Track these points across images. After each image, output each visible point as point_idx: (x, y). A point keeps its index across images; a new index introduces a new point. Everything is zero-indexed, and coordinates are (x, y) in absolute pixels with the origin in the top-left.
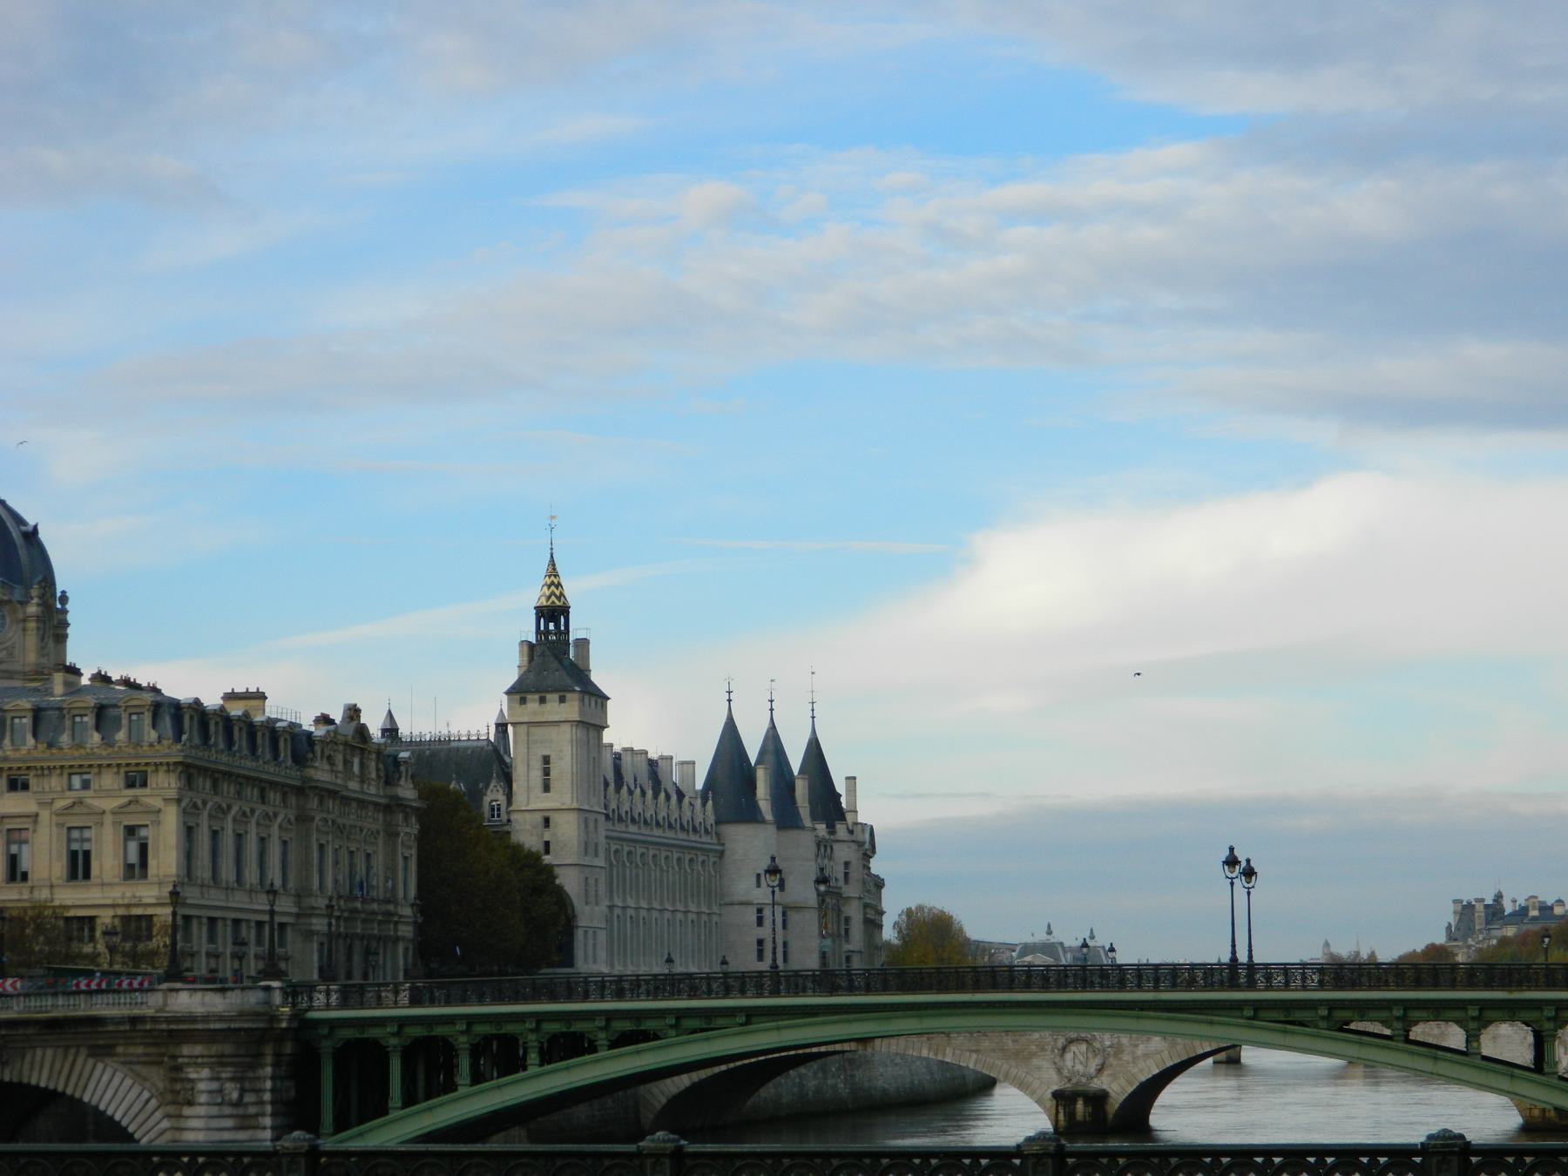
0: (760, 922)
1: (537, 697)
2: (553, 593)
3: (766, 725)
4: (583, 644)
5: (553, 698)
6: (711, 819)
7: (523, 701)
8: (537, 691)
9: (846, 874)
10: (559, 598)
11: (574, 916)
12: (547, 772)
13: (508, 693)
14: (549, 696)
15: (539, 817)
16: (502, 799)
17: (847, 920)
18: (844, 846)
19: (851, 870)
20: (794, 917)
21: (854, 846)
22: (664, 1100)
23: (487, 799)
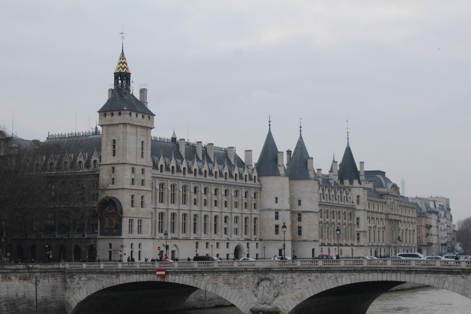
0: (277, 218)
1: (110, 113)
2: (121, 67)
3: (298, 137)
4: (143, 91)
5: (116, 113)
6: (255, 174)
7: (105, 115)
8: (110, 111)
10: (123, 69)
11: (122, 212)
12: (114, 146)
13: (99, 112)
14: (114, 113)
15: (110, 167)
16: (98, 159)
17: (358, 219)
18: (357, 189)
20: (304, 216)
21: (362, 189)
22: (76, 304)
23: (92, 160)
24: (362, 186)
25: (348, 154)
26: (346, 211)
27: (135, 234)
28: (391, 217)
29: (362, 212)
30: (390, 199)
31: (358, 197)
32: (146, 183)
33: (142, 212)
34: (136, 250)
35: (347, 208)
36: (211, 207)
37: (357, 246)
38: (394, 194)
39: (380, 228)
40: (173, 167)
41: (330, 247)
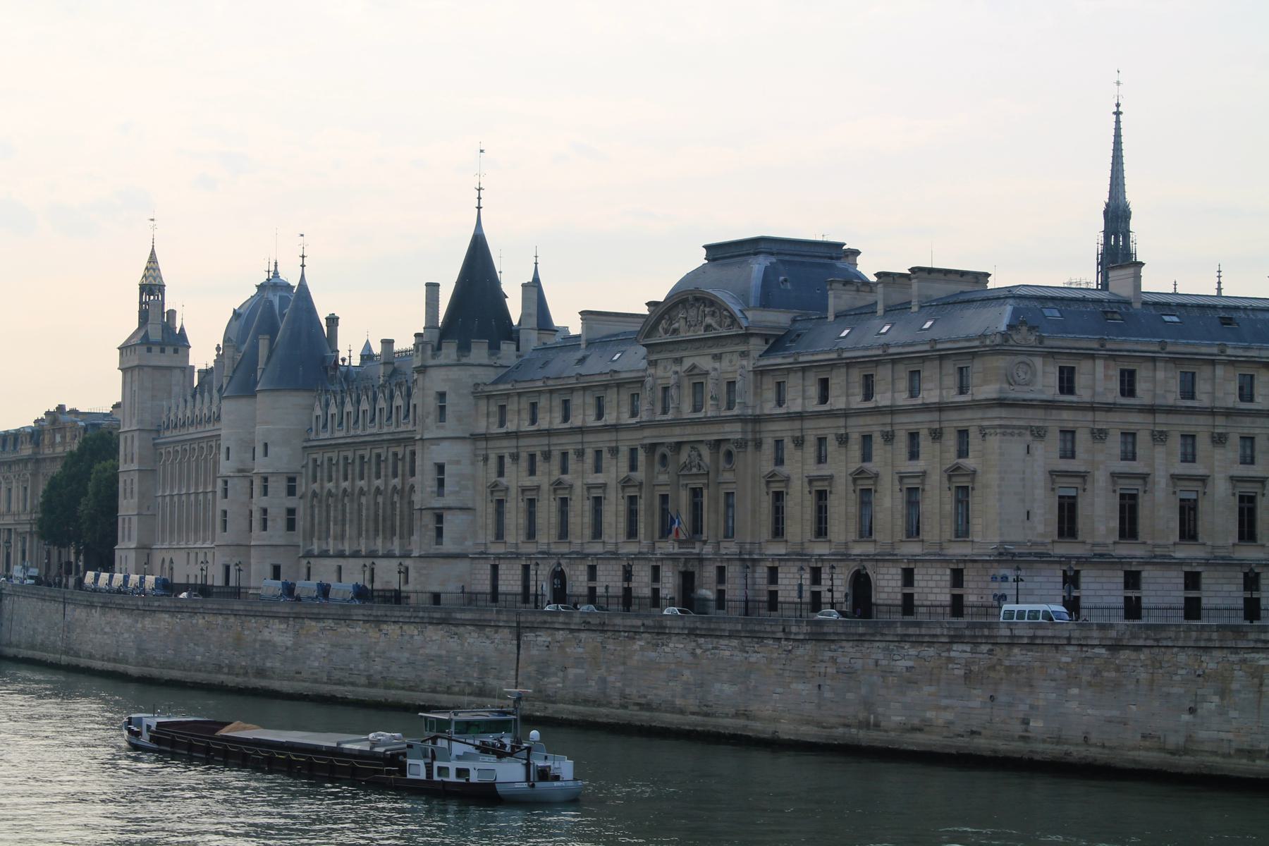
30: (679, 361)
39: (604, 486)
41: (341, 562)
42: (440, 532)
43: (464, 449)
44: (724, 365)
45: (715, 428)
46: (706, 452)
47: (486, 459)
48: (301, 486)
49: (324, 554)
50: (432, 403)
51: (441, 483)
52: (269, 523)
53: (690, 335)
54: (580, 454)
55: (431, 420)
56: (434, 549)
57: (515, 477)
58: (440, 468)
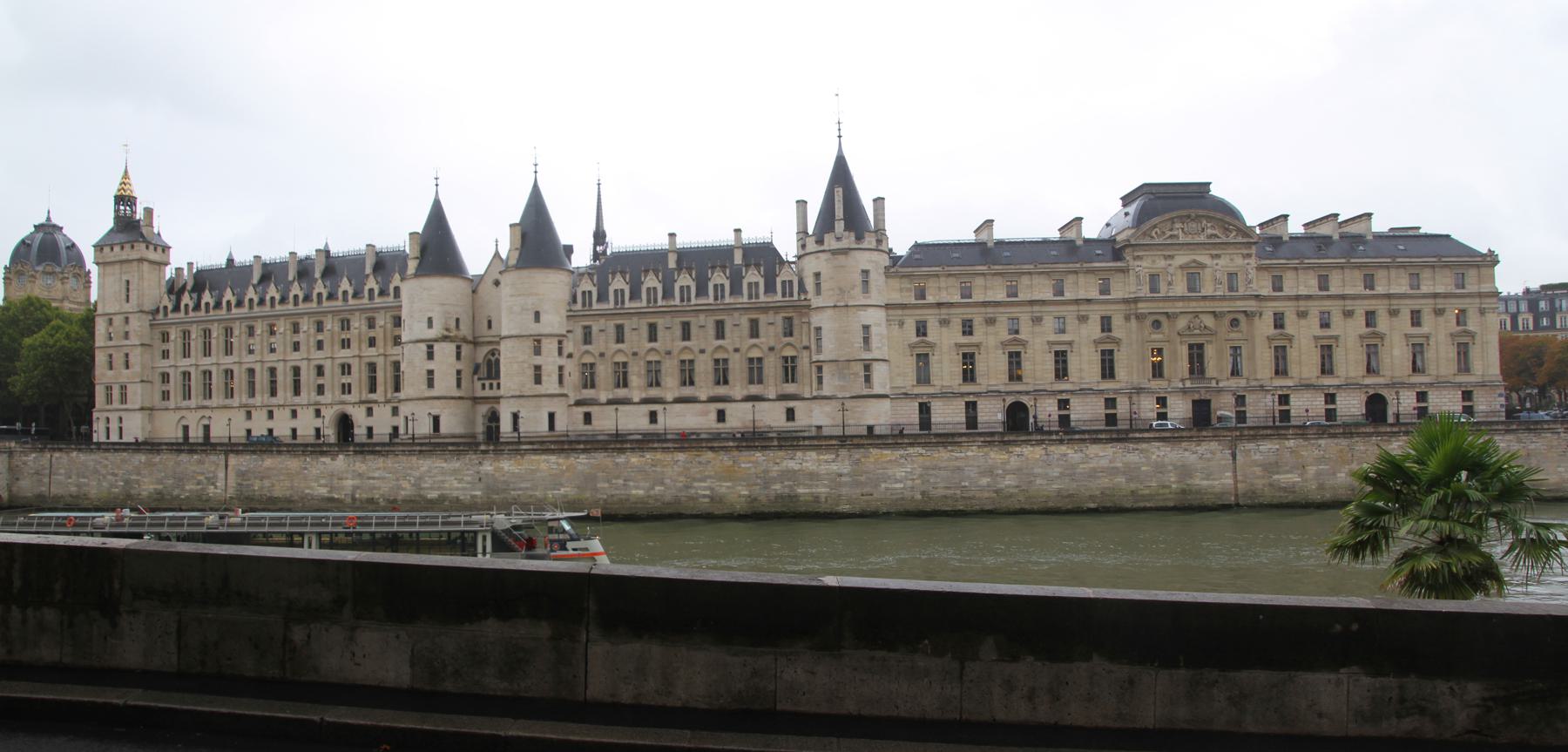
9: (818, 285)
17: (818, 329)
19: (823, 277)
24: (825, 247)
25: (841, 175)
26: (763, 319)
27: (116, 405)
28: (1143, 308)
29: (830, 312)
31: (817, 275)
32: (131, 335)
33: (125, 375)
34: (114, 426)
35: (765, 309)
36: (285, 352)
37: (815, 398)
38: (1202, 239)
39: (1070, 343)
40: (251, 300)
42: (868, 379)
43: (882, 314)
44: (1222, 262)
45: (1225, 303)
46: (1209, 321)
47: (901, 324)
48: (569, 347)
49: (626, 402)
50: (859, 279)
51: (866, 340)
52: (544, 378)
53: (1189, 240)
54: (1037, 320)
55: (859, 289)
56: (866, 392)
57: (946, 339)
58: (866, 328)
